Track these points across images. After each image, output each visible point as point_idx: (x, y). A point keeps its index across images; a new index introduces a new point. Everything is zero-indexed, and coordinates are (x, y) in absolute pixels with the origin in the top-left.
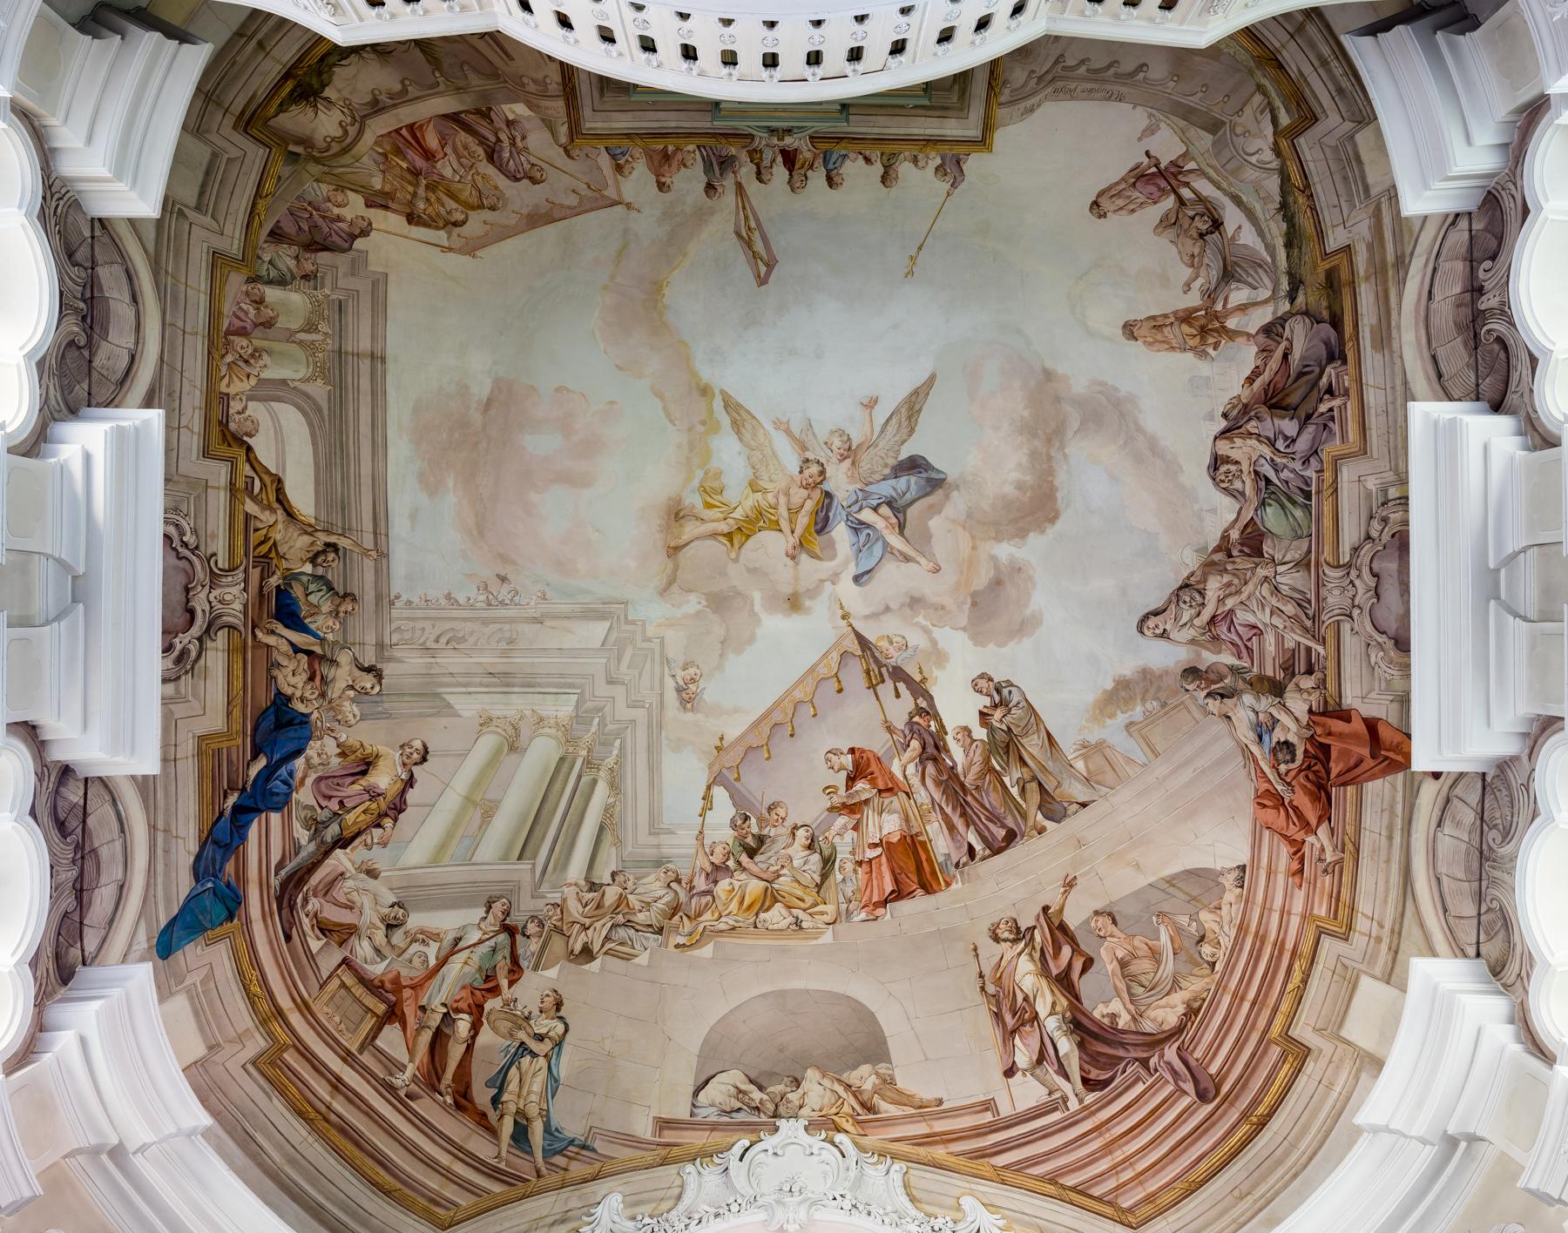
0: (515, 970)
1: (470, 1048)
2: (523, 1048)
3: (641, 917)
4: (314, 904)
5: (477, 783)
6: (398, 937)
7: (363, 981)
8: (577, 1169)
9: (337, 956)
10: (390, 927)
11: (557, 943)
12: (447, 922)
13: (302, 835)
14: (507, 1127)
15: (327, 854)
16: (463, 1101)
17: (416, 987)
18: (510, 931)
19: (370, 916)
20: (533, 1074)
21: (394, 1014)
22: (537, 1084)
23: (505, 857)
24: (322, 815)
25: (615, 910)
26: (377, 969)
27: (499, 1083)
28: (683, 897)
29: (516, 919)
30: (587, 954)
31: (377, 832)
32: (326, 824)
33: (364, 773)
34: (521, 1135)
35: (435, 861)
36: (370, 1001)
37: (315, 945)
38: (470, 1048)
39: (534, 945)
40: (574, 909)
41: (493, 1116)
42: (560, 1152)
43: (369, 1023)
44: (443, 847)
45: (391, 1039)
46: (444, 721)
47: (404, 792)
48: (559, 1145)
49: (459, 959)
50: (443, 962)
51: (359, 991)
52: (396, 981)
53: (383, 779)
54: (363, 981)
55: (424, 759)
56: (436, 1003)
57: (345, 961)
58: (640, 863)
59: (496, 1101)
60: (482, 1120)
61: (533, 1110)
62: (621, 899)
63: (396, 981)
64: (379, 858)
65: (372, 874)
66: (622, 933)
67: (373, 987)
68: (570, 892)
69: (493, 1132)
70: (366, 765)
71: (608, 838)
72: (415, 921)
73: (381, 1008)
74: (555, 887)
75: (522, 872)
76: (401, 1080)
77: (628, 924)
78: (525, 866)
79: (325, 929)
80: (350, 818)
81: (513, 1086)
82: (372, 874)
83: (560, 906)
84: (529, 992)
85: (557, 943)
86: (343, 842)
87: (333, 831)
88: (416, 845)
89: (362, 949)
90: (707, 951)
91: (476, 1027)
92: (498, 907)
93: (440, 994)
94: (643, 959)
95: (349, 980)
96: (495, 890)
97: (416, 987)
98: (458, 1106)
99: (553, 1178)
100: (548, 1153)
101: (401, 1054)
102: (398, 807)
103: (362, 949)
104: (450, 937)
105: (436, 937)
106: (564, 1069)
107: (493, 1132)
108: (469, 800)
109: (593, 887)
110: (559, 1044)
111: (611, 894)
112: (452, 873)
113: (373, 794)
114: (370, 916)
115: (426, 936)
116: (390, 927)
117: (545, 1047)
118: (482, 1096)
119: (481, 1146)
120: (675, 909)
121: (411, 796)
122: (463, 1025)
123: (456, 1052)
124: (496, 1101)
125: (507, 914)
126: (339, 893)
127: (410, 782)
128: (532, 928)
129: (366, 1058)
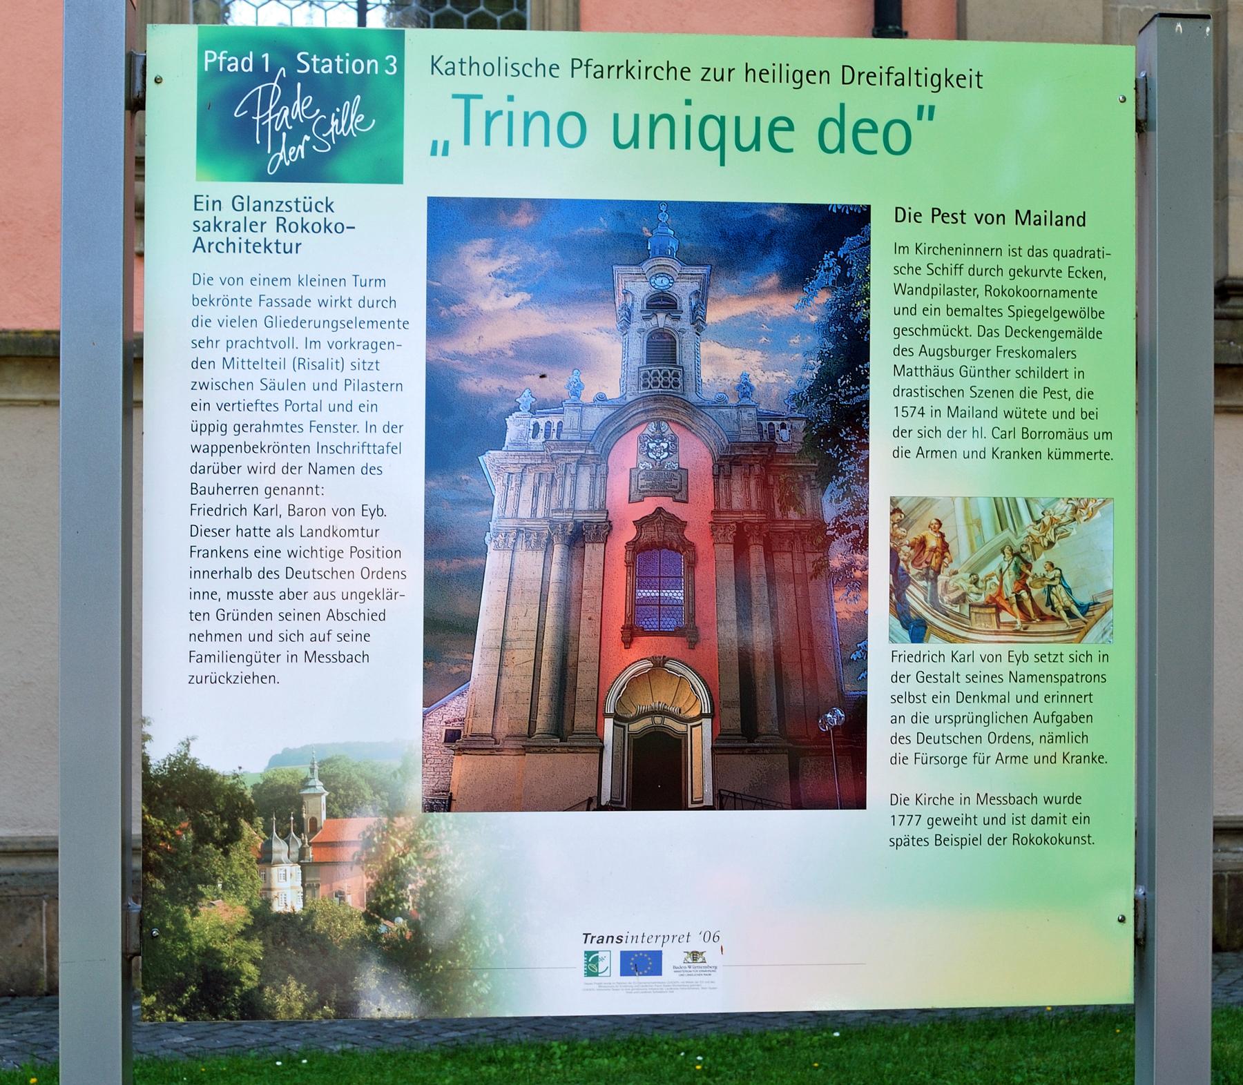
0: (1029, 566)
1: (1032, 599)
2: (1050, 587)
3: (1064, 520)
4: (946, 598)
5: (966, 517)
6: (980, 584)
7: (981, 606)
8: (1097, 613)
9: (967, 607)
10: (975, 583)
11: (1037, 547)
12: (993, 567)
13: (923, 583)
14: (1064, 615)
15: (936, 581)
16: (1043, 618)
17: (1000, 594)
18: (1017, 555)
19: (966, 585)
20: (1059, 591)
21: (999, 608)
22: (1063, 594)
23: (997, 533)
24: (924, 572)
25: (1052, 523)
26: (982, 599)
27: (1050, 602)
28: (1076, 503)
29: (1016, 549)
30: (1051, 544)
31: (946, 560)
32: (927, 573)
33: (925, 547)
34: (1070, 614)
35: (973, 552)
36: (988, 611)
37: (957, 610)
38: (1032, 599)
39: (1029, 553)
40: (1036, 533)
41: (1056, 614)
42: (1088, 611)
43: (994, 618)
44: (972, 546)
45: (1005, 617)
46: (935, 507)
47: (943, 541)
48: (1084, 609)
49: (1006, 576)
50: (1001, 580)
51: (982, 611)
52: (991, 597)
53: (933, 542)
54: (981, 606)
55: (940, 524)
56: (1010, 594)
57: (971, 606)
58: (1050, 503)
59: (1053, 609)
60: (1053, 618)
61: (1068, 603)
62: (1051, 520)
63: (991, 597)
64: (953, 567)
65: (956, 573)
66: (1059, 530)
67: (986, 606)
68: (1031, 530)
69: (1060, 619)
70: (923, 542)
71: (1032, 503)
72: (982, 575)
73: (994, 610)
74: (1023, 531)
75: (1007, 534)
76: (1018, 626)
77: (1060, 526)
78: (1006, 531)
79: (955, 602)
80: (933, 564)
81: (1055, 600)
82: (956, 573)
83: (1030, 535)
84: (1039, 568)
85: (1037, 547)
86: (938, 572)
87: (931, 572)
88: (961, 552)
89: (973, 598)
90: (1098, 515)
91: (1029, 592)
92: (1006, 550)
93: (1009, 591)
94: (1074, 532)
95: (976, 610)
96: (1001, 546)
97: (1000, 594)
98: (1043, 620)
99: (1092, 620)
100: (1083, 614)
101: (1012, 619)
102: (945, 547)
103: (973, 598)
104: (998, 572)
105: (993, 574)
106: (1069, 583)
107: (1060, 619)
108: (968, 525)
109: (1038, 522)
110: (1061, 577)
111: (1047, 520)
112: (981, 552)
113: (934, 550)
114: (966, 585)
115: (989, 577)
116: (975, 583)
117: (1057, 580)
118: (1048, 611)
119: (1060, 627)
120: (1075, 509)
121: (947, 540)
122: (1024, 594)
123: (1028, 604)
124: (1053, 609)
125: (1011, 550)
126: (951, 588)
127: (943, 536)
128: (1024, 549)
129: (1002, 628)
